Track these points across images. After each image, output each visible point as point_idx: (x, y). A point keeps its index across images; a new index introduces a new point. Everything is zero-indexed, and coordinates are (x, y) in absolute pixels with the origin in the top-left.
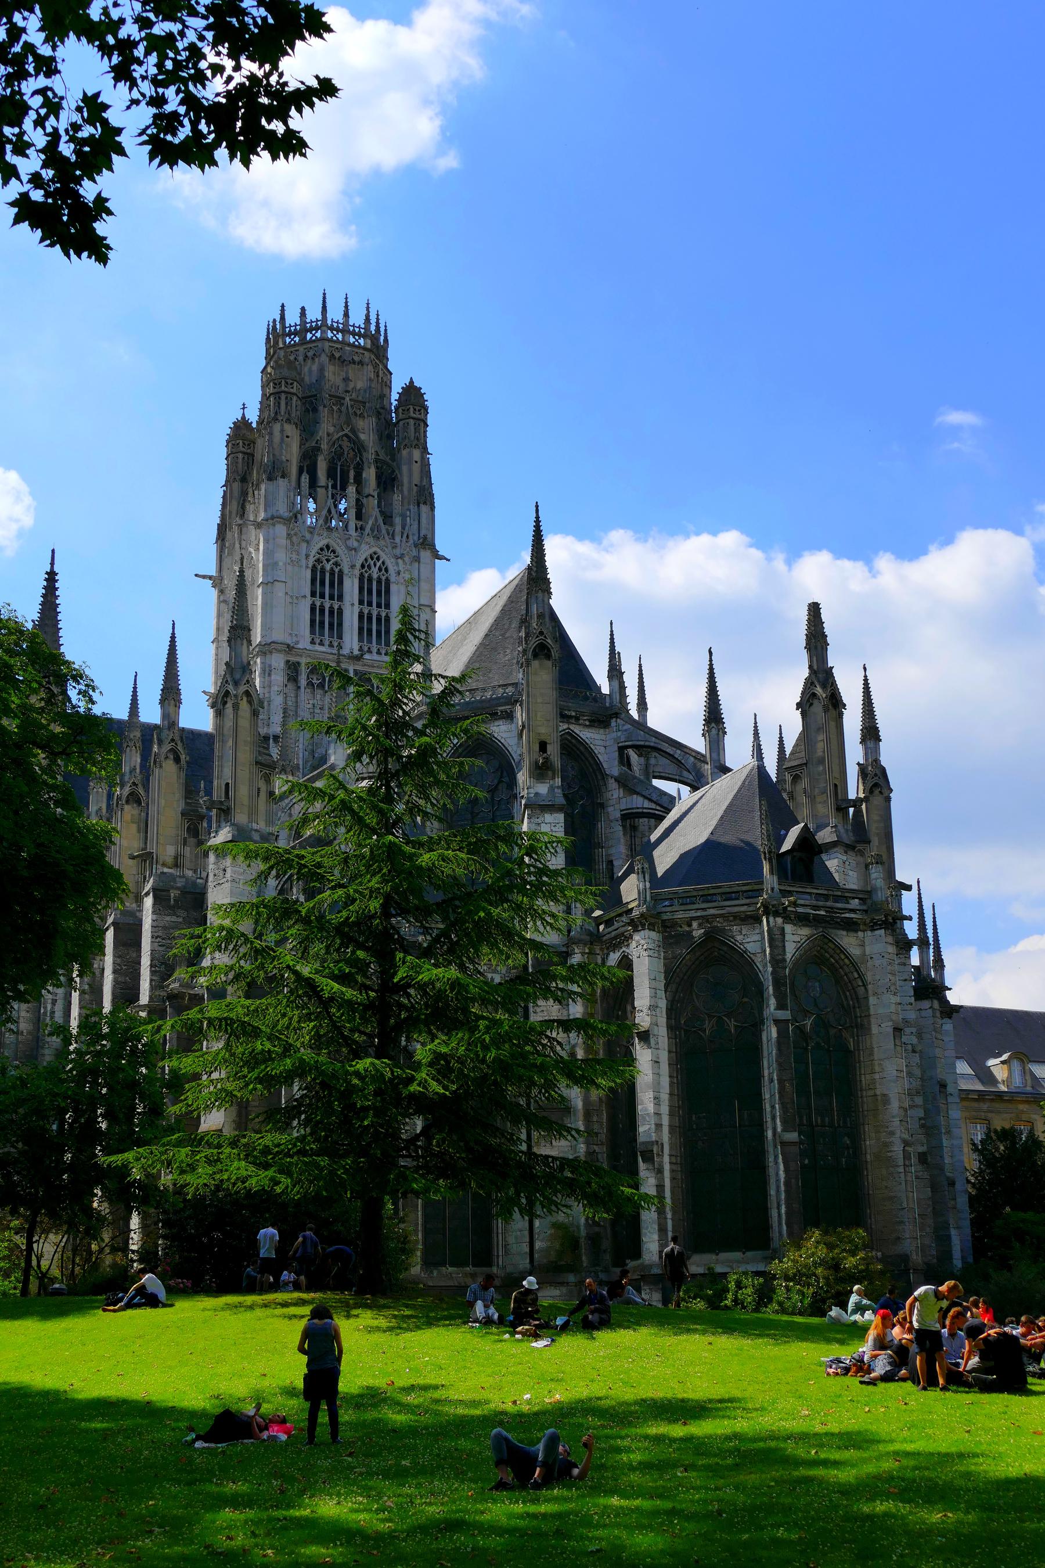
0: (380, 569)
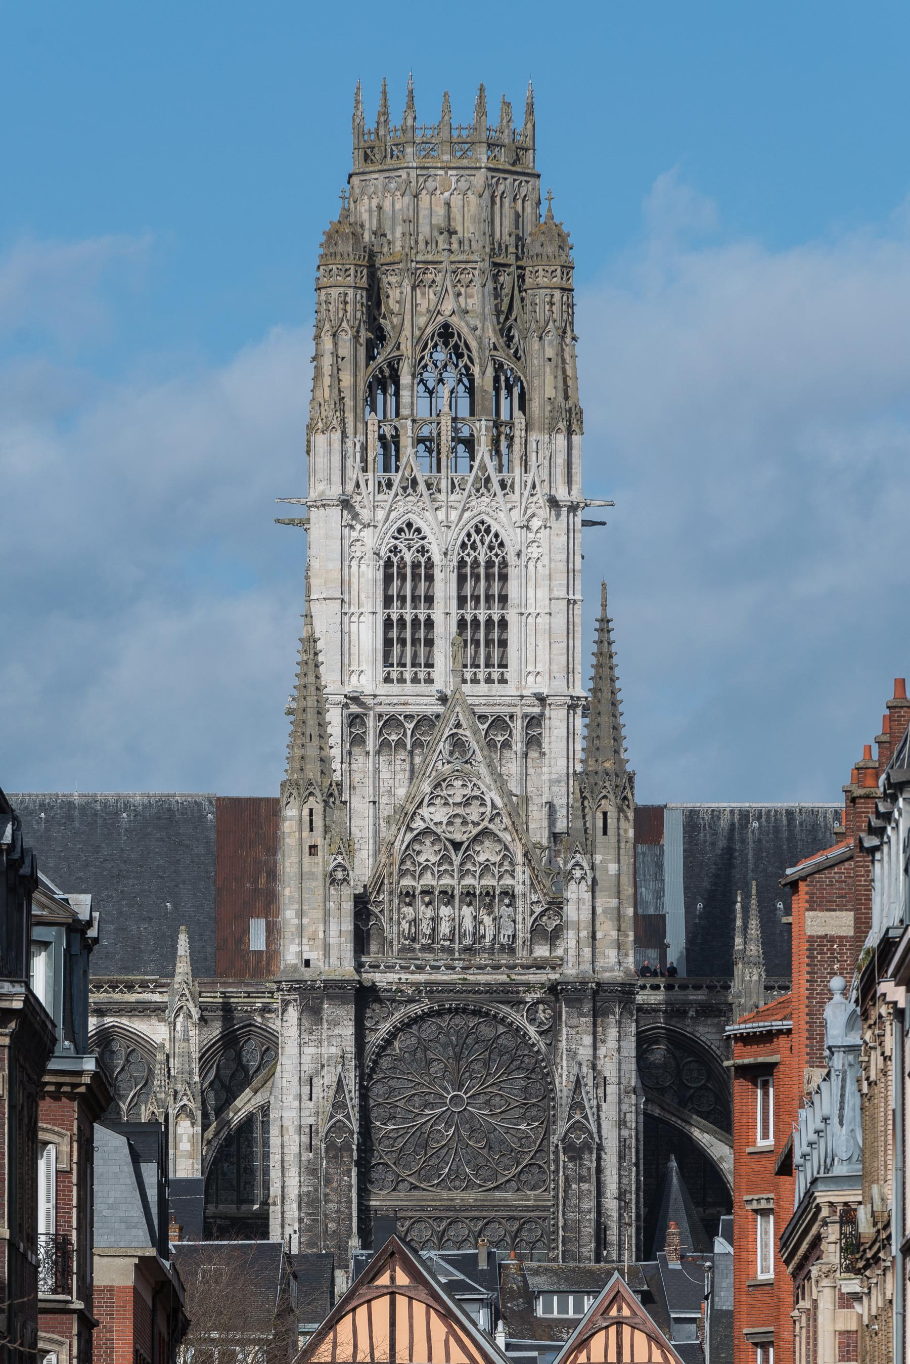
0: (491, 548)
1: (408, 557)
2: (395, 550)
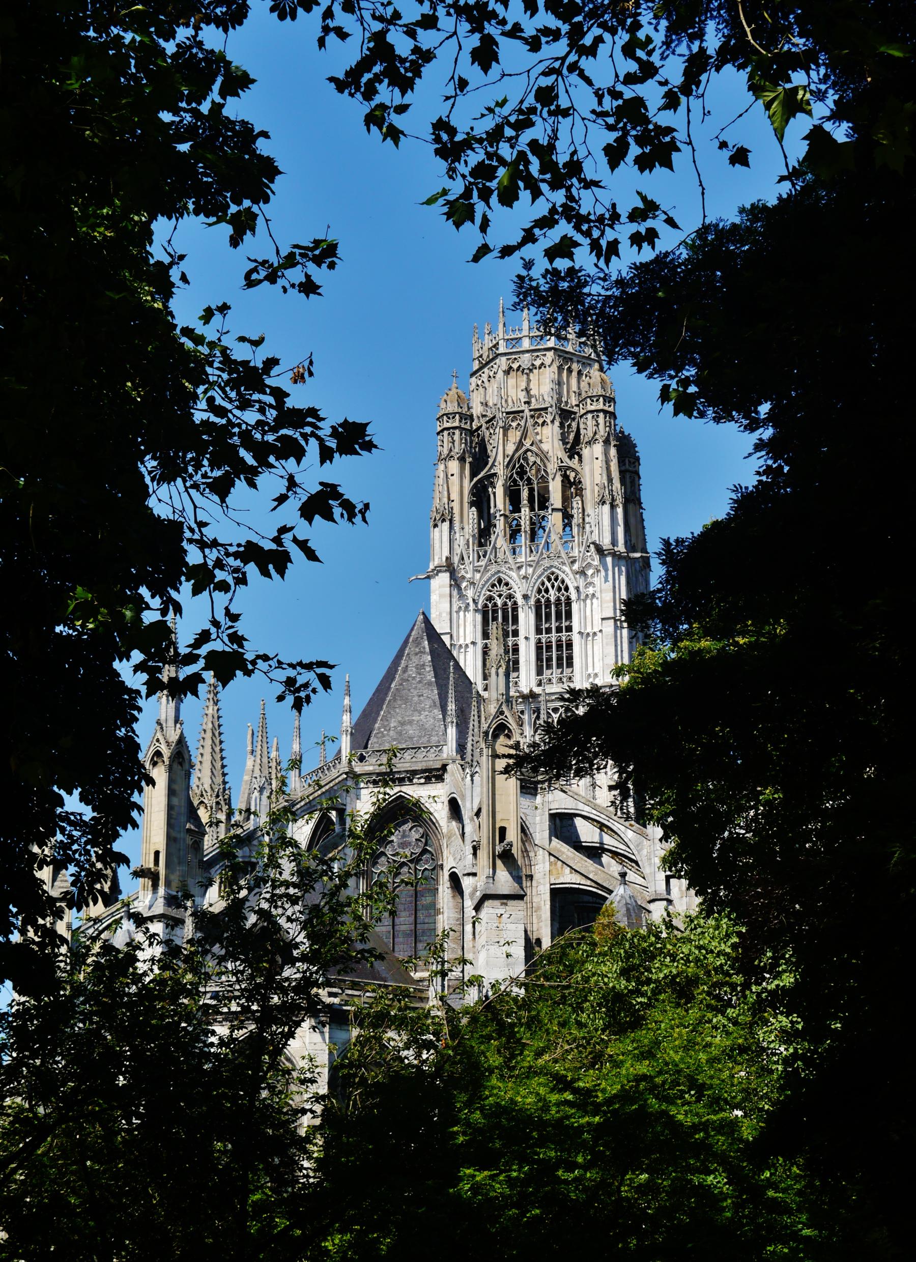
0: (559, 589)
1: (499, 602)
2: (490, 598)
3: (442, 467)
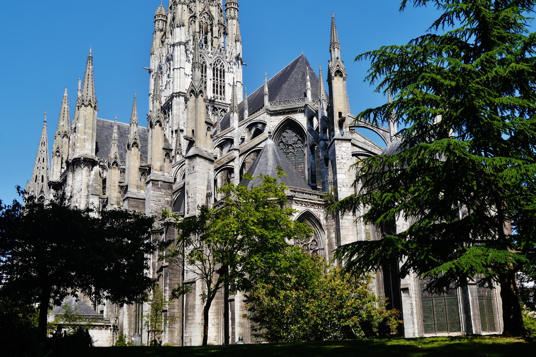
0: (221, 66)
3: (179, 6)
